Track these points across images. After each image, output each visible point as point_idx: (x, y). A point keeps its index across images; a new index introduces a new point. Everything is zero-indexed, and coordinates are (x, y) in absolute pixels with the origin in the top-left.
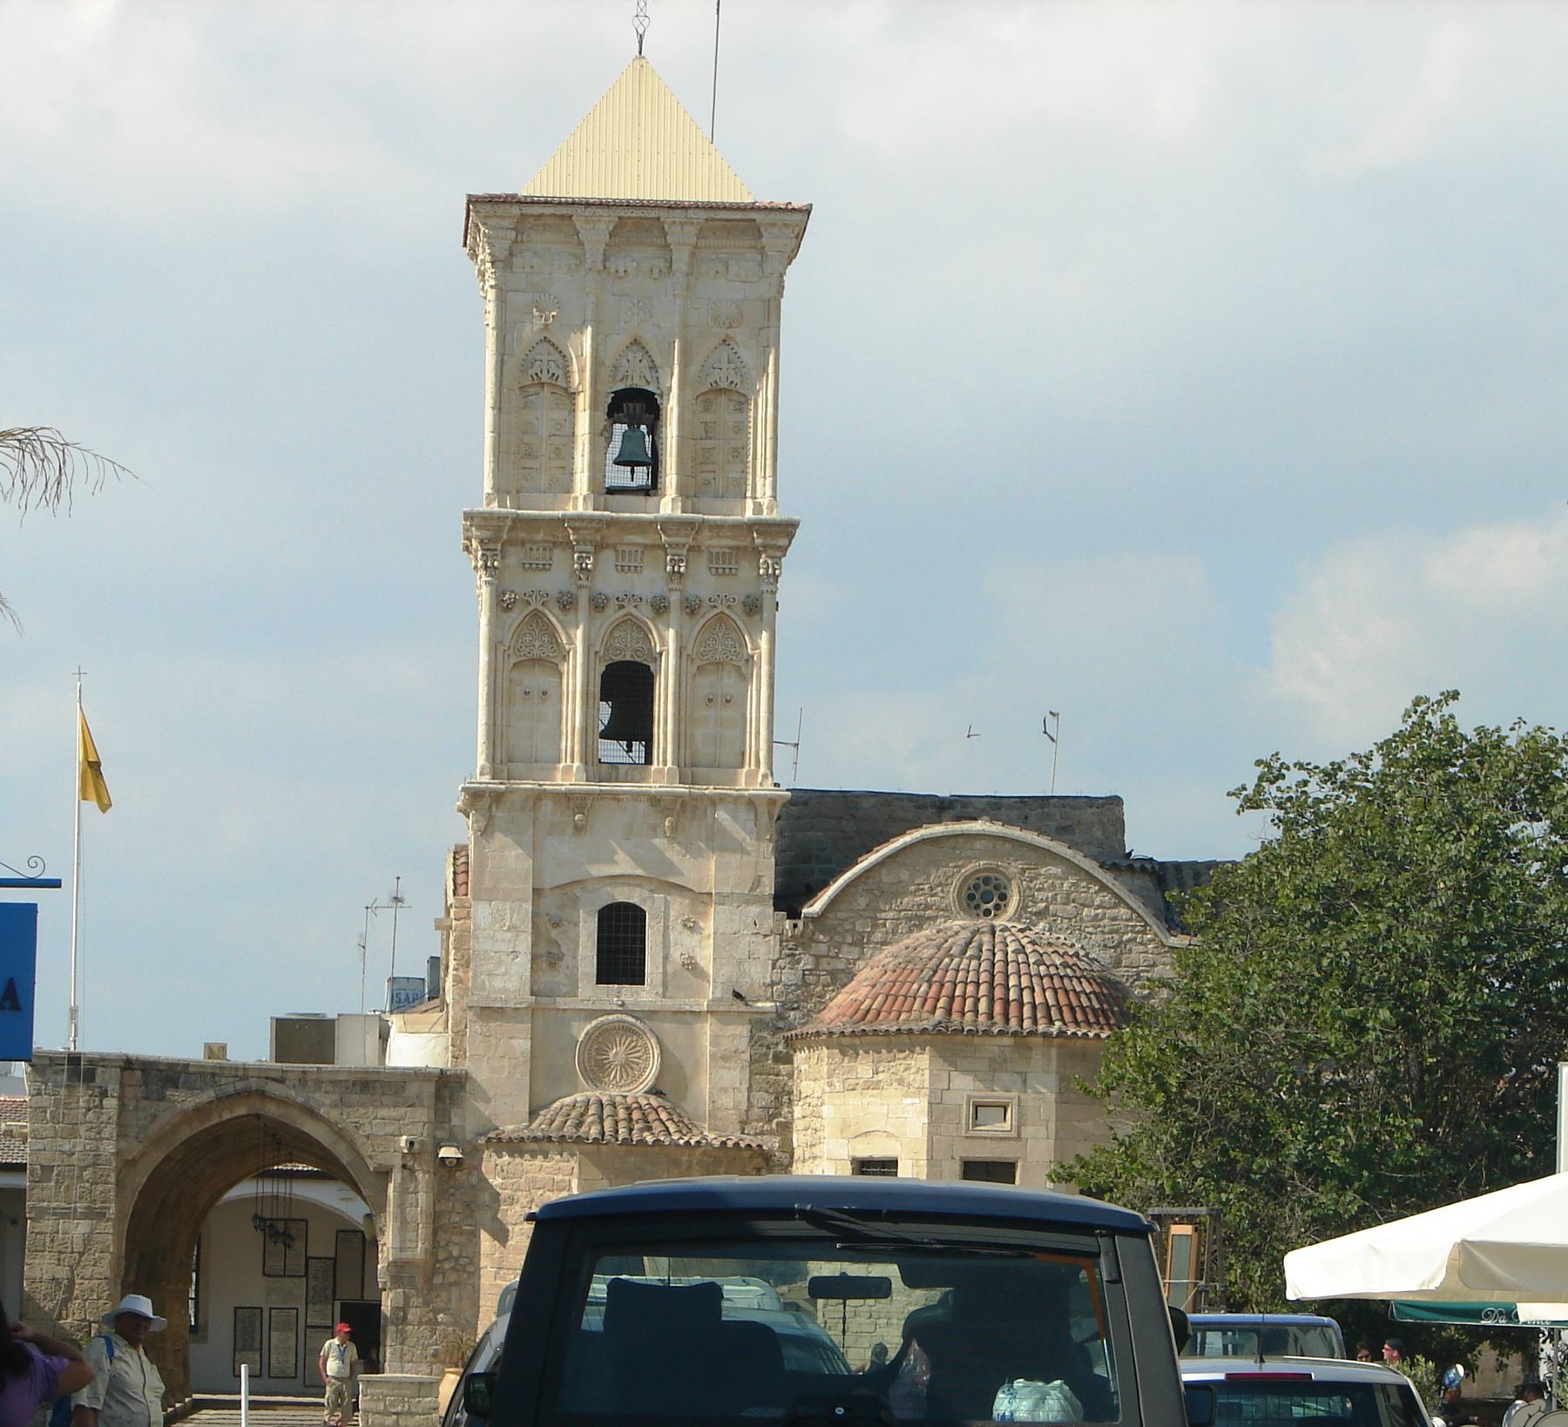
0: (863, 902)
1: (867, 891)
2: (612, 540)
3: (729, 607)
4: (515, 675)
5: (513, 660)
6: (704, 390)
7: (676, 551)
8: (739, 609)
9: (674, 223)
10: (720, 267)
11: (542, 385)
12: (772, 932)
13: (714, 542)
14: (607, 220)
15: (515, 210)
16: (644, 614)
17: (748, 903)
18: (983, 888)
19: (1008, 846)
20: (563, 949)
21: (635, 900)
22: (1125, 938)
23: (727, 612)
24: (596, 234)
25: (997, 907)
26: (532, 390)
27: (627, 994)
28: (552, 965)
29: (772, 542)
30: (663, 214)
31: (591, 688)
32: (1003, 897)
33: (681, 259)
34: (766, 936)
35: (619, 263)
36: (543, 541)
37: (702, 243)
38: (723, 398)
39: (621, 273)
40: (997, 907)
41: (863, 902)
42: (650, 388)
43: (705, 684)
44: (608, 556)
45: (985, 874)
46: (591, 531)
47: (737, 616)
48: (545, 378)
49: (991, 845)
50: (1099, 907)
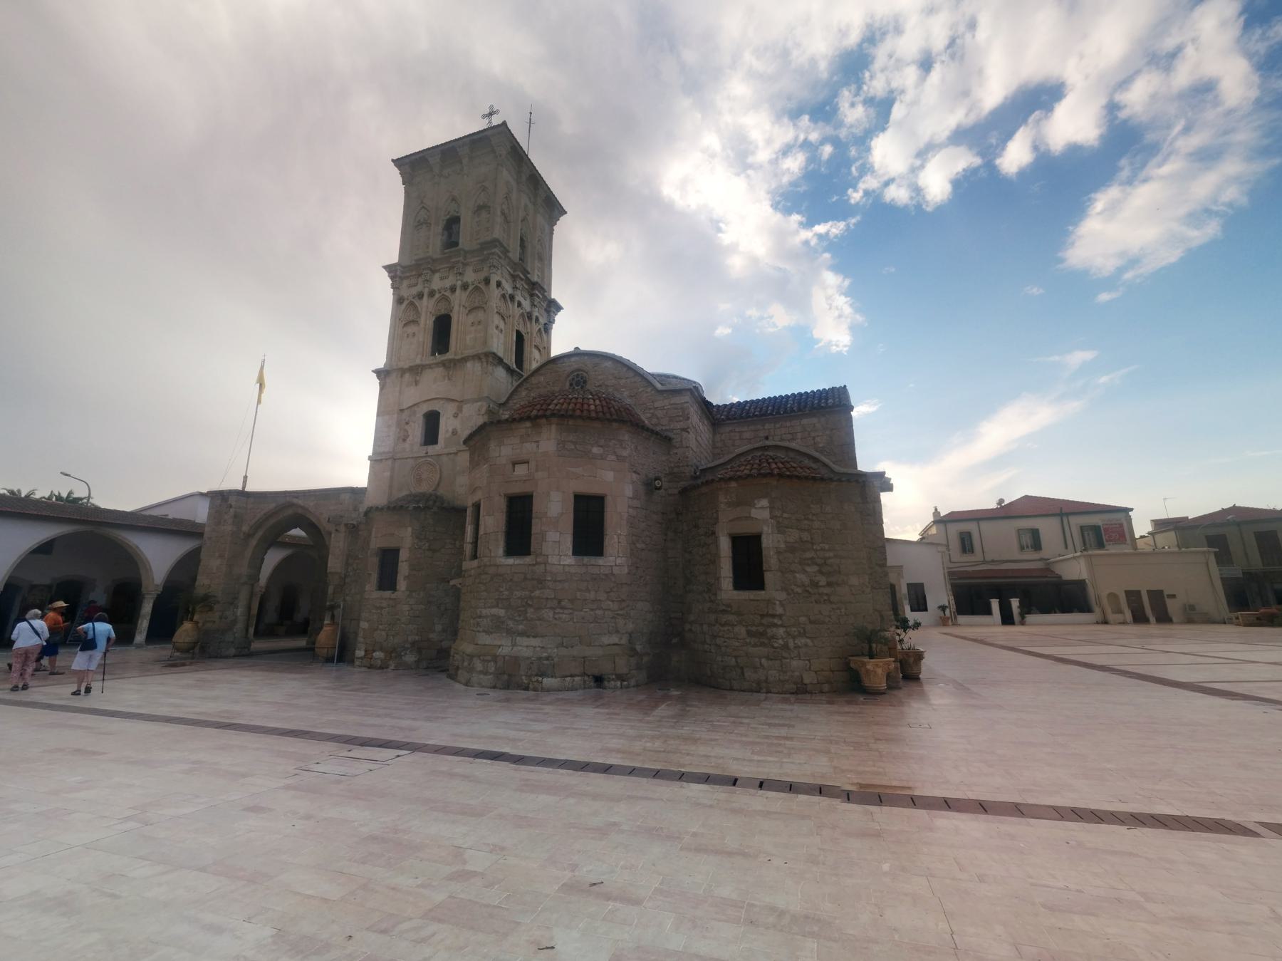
0: (524, 394)
1: (527, 389)
2: (438, 268)
4: (405, 329)
5: (404, 322)
11: (422, 224)
12: (486, 413)
13: (472, 260)
16: (448, 293)
17: (477, 402)
19: (586, 358)
20: (409, 433)
21: (437, 409)
22: (640, 390)
23: (478, 285)
26: (419, 227)
27: (432, 449)
28: (404, 440)
31: (427, 326)
33: (465, 161)
34: (483, 415)
36: (415, 275)
41: (524, 394)
42: (459, 214)
43: (471, 318)
44: (437, 275)
45: (576, 374)
47: (482, 286)
48: (422, 220)
50: (627, 378)
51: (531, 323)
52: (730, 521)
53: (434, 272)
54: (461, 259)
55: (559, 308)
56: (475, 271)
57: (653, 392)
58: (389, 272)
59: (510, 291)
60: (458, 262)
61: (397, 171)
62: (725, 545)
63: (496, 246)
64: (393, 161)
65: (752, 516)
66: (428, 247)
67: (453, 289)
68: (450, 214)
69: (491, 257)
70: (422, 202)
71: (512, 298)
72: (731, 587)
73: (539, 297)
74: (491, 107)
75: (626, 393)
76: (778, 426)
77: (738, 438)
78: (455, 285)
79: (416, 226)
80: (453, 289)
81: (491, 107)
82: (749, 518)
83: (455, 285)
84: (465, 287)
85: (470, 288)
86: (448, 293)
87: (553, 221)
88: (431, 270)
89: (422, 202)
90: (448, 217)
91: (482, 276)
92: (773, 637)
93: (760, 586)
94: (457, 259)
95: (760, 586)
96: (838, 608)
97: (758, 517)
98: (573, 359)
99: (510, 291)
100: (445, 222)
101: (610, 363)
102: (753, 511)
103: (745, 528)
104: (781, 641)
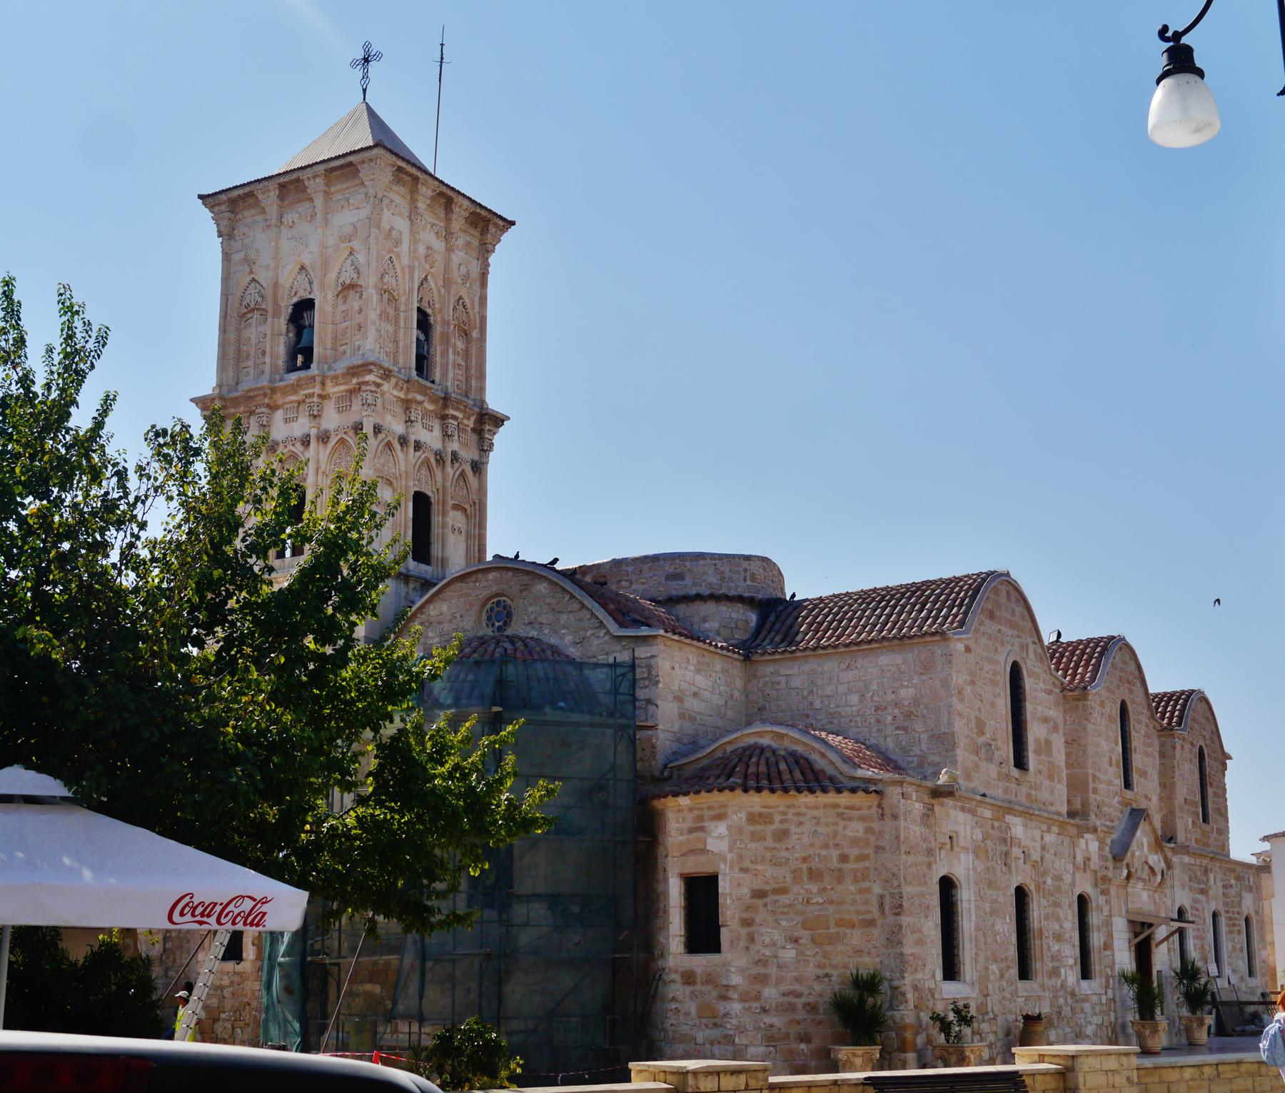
3: (345, 433)
6: (340, 289)
7: (311, 400)
8: (352, 433)
9: (309, 179)
10: (343, 202)
11: (253, 310)
13: (336, 389)
14: (272, 185)
15: (224, 197)
18: (496, 609)
19: (510, 574)
22: (589, 633)
23: (345, 436)
24: (270, 199)
25: (505, 623)
26: (249, 315)
29: (361, 380)
30: (300, 174)
32: (509, 615)
35: (290, 217)
37: (333, 189)
38: (352, 293)
39: (291, 223)
40: (505, 623)
44: (279, 415)
45: (495, 600)
46: (261, 398)
49: (498, 575)
51: (443, 468)
52: (683, 855)
53: (273, 408)
54: (317, 390)
55: (499, 421)
56: (340, 411)
57: (607, 638)
58: (203, 409)
59: (399, 428)
60: (311, 395)
61: (206, 214)
62: (675, 892)
63: (370, 371)
64: (200, 197)
65: (708, 848)
66: (264, 353)
67: (306, 442)
68: (298, 295)
69: (363, 388)
70: (251, 272)
71: (403, 441)
72: (681, 949)
73: (455, 418)
74: (367, 46)
75: (569, 638)
76: (843, 666)
77: (783, 685)
78: (308, 435)
79: (244, 315)
80: (306, 442)
81: (367, 46)
82: (704, 851)
83: (308, 435)
84: (324, 438)
85: (333, 441)
86: (298, 448)
87: (485, 250)
88: (268, 406)
89: (251, 272)
90: (295, 300)
91: (352, 418)
92: (726, 1015)
93: (715, 948)
94: (311, 391)
95: (715, 948)
96: (827, 975)
97: (716, 851)
98: (491, 576)
99: (399, 428)
100: (290, 310)
101: (545, 584)
102: (709, 841)
103: (696, 866)
104: (734, 1021)
